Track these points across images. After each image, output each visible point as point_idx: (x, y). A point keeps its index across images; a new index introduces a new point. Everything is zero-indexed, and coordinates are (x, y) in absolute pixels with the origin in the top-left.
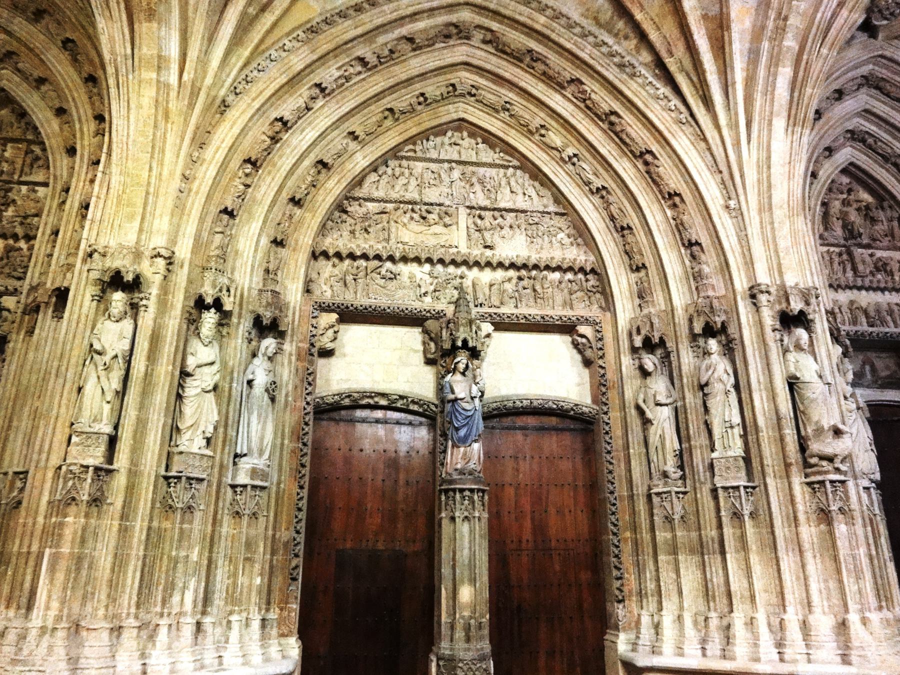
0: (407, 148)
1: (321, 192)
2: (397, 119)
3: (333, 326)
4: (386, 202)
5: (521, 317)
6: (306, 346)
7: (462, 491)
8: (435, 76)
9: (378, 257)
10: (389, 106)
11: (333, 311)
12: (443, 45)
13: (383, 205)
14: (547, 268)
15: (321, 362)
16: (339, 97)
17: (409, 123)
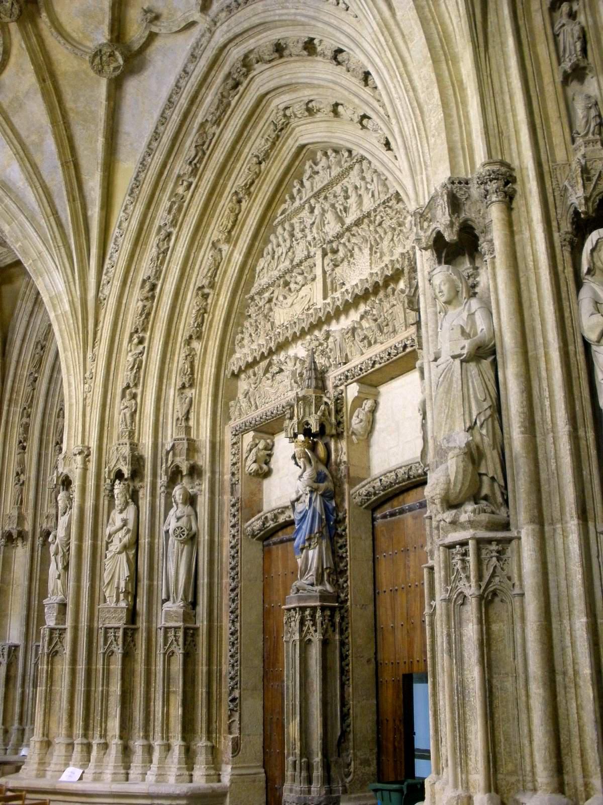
0: (279, 212)
1: (217, 313)
2: (249, 194)
3: (257, 445)
6: (227, 477)
7: (289, 610)
8: (254, 127)
9: (263, 358)
10: (233, 191)
11: (246, 431)
12: (237, 97)
15: (266, 482)
16: (187, 219)
17: (264, 187)
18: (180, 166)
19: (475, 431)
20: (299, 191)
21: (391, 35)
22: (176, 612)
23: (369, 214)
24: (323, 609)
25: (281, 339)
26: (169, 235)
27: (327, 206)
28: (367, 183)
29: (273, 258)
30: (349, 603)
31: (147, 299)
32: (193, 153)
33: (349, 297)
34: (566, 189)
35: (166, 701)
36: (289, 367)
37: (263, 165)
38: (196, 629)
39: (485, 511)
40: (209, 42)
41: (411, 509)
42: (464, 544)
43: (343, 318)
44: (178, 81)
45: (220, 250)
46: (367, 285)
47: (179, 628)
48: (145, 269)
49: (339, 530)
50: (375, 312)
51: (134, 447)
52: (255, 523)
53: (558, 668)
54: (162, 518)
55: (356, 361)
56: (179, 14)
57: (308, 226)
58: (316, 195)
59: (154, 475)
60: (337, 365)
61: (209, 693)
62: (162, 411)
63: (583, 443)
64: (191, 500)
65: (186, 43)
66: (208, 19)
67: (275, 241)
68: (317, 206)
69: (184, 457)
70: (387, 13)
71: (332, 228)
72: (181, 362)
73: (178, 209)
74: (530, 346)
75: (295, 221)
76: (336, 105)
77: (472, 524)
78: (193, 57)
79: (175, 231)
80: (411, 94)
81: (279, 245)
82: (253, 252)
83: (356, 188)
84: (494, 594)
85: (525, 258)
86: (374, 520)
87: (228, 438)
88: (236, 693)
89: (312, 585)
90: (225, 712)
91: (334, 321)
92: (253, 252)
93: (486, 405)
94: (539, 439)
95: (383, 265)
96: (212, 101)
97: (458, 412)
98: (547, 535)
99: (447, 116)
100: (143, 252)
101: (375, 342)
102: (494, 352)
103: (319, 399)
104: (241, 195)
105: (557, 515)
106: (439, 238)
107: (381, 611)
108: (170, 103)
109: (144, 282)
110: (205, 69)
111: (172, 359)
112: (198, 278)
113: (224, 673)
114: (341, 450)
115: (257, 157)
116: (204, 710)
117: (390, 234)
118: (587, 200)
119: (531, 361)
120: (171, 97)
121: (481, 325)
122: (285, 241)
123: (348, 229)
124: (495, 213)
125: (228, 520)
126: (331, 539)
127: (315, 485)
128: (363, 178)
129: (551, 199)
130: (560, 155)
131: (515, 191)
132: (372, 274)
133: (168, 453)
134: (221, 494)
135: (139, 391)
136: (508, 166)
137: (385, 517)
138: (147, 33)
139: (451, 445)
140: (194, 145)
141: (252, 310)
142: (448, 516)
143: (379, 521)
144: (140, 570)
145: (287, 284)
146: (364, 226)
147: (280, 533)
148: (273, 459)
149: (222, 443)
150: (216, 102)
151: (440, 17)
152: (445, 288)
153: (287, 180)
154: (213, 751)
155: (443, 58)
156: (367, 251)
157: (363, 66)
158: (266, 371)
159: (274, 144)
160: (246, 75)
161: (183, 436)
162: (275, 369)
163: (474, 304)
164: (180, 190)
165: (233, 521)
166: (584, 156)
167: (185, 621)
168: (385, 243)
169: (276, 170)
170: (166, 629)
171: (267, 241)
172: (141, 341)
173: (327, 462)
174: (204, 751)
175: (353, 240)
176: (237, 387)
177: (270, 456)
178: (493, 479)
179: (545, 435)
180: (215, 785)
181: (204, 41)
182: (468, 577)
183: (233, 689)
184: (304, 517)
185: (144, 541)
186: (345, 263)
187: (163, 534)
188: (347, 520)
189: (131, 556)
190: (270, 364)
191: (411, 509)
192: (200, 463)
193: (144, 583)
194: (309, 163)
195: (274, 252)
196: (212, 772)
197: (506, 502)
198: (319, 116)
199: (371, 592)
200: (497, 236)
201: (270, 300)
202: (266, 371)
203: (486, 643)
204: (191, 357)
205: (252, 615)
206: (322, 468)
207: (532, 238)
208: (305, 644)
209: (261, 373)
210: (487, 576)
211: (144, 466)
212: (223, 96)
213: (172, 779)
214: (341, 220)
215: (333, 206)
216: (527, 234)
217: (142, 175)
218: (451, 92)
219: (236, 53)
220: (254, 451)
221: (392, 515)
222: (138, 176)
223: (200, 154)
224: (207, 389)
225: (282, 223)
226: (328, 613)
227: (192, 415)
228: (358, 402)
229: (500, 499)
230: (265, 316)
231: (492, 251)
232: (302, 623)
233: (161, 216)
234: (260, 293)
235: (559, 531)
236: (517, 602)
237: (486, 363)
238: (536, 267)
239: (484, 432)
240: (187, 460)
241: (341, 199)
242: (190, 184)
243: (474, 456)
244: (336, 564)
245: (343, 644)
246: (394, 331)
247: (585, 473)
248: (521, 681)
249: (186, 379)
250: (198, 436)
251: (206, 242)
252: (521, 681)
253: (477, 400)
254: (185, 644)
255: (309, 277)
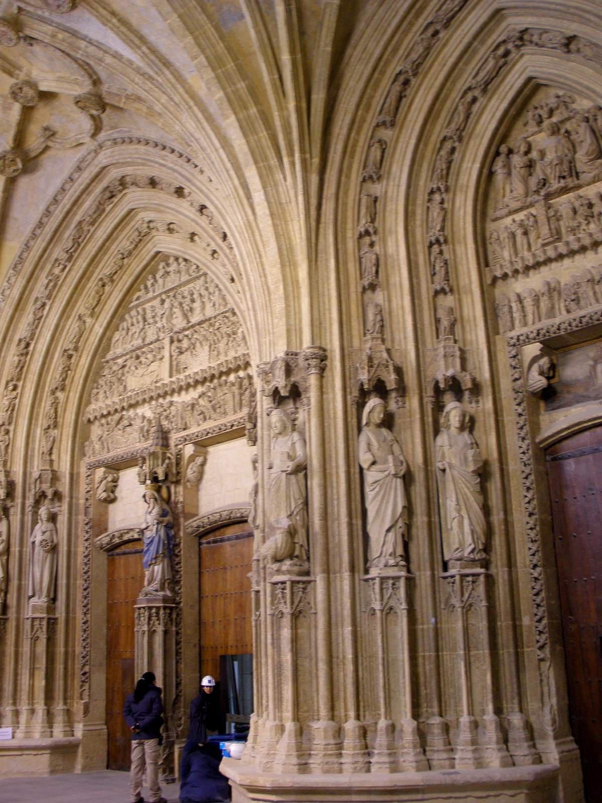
0: (135, 297)
1: (78, 370)
2: (112, 281)
3: (106, 478)
4: (127, 354)
5: (205, 433)
6: (82, 501)
7: (139, 608)
8: (122, 230)
9: (116, 411)
11: (99, 467)
12: (111, 206)
13: (124, 358)
14: (221, 374)
15: (111, 506)
16: (60, 294)
17: (125, 277)
18: (58, 252)
19: (293, 517)
20: (153, 285)
21: (253, 233)
22: (41, 606)
23: (210, 319)
24: (165, 608)
25: (133, 402)
26: (44, 305)
27: (176, 304)
28: (210, 293)
29: (127, 334)
30: (182, 605)
31: (22, 355)
32: (70, 244)
33: (191, 381)
34: (357, 369)
35: (32, 675)
36: (137, 424)
37: (126, 261)
38: (56, 619)
39: (296, 565)
40: (93, 159)
41: (229, 539)
42: (283, 583)
43: (183, 393)
44: (64, 185)
45: (84, 322)
46: (205, 375)
47: (43, 618)
48: (22, 330)
49: (177, 551)
50: (210, 394)
51: (7, 474)
52: (104, 539)
53: (334, 655)
54: (29, 531)
55: (194, 430)
56: (72, 134)
57: (159, 314)
58: (165, 292)
59: (24, 497)
60: (178, 430)
61: (66, 669)
62: (30, 446)
63: (355, 528)
64: (53, 518)
65: (72, 159)
66: (96, 143)
67: (130, 321)
68: (168, 301)
69: (49, 485)
70: (251, 218)
71: (179, 322)
72: (48, 408)
73: (54, 286)
74: (328, 466)
75: (147, 306)
76: (193, 235)
77: (289, 572)
78: (79, 169)
79: (49, 303)
80: (263, 279)
81: (133, 325)
82: (112, 326)
83: (201, 295)
84: (300, 612)
85: (329, 411)
86: (200, 544)
87: (83, 471)
88: (87, 669)
89: (157, 591)
90: (77, 683)
91: (176, 394)
92: (112, 326)
93: (300, 502)
94: (329, 523)
95: (219, 362)
96: (91, 205)
97: (283, 505)
98: (331, 580)
99: (287, 306)
100: (20, 316)
101: (210, 418)
102: (305, 468)
103: (164, 454)
104: (106, 281)
105: (337, 568)
106: (276, 392)
107: (204, 610)
108: (55, 201)
109: (20, 341)
110: (88, 181)
111: (40, 405)
112: (65, 341)
113: (77, 652)
114: (179, 493)
115: (122, 254)
116: (62, 682)
117: (225, 340)
118: (369, 380)
119: (328, 475)
120: (56, 196)
121: (299, 452)
122: (138, 322)
123: (193, 326)
124: (313, 381)
125: (82, 536)
126: (170, 558)
127: (161, 519)
128: (207, 289)
129: (347, 374)
130: (356, 343)
131: (326, 365)
132: (210, 367)
133: (36, 480)
134: (77, 515)
135: (12, 428)
136: (325, 350)
137: (208, 543)
138: (43, 146)
139: (279, 526)
140: (72, 238)
141: (106, 372)
142: (275, 566)
143: (205, 545)
144: (11, 572)
145: (138, 357)
146: (205, 325)
147: (123, 547)
148: (118, 490)
149: (78, 474)
150: (94, 207)
151: (288, 233)
152: (278, 425)
153: (144, 274)
154: (68, 713)
155: (287, 264)
156: (207, 348)
157: (222, 228)
158: (118, 423)
159: (136, 246)
160: (121, 191)
161: (48, 468)
162: (126, 422)
163: (296, 436)
164: (57, 271)
165: (87, 536)
166: (371, 349)
167: (48, 613)
168: (222, 346)
169: (135, 266)
170: (33, 619)
171: (123, 319)
172: (15, 388)
173: (168, 501)
174: (61, 713)
175: (196, 336)
176: (89, 432)
177: (116, 486)
178: (302, 546)
179: (333, 521)
180: (71, 738)
181: (89, 157)
182: (285, 602)
183: (84, 665)
184: (152, 541)
185: (15, 549)
186: (189, 353)
187: (30, 544)
188: (182, 545)
189: (4, 561)
190: (121, 418)
191: (229, 539)
192: (60, 489)
193: (14, 583)
194: (162, 265)
195: (128, 329)
196: (68, 729)
197: (308, 558)
198: (176, 235)
199: (197, 597)
200: (313, 395)
201: (124, 366)
202: (118, 423)
203: (295, 640)
204: (55, 404)
205: (99, 608)
206: (166, 507)
207: (334, 398)
208: (152, 633)
209: (113, 423)
210: (296, 601)
211: (14, 490)
212: (100, 204)
213: (37, 735)
214: (185, 316)
215: (181, 304)
216: (331, 396)
217: (25, 255)
218: (291, 289)
219: (114, 174)
220: (104, 482)
221: (215, 542)
222: (21, 254)
223: (76, 246)
224: (68, 431)
225: (137, 306)
226: (168, 611)
227: (55, 451)
228: (192, 458)
229: (305, 557)
230: (119, 379)
231: (309, 405)
232: (150, 619)
233: (39, 289)
234: (113, 359)
235: (338, 578)
236: (313, 617)
237: (301, 475)
238: (335, 418)
239: (298, 518)
240: (51, 487)
241: (188, 300)
242: (65, 267)
243: (291, 533)
244: (174, 577)
245: (177, 633)
246: (225, 413)
247: (355, 545)
248: (314, 662)
249: (51, 422)
250: (59, 467)
251: (74, 313)
252: (314, 662)
253: (295, 499)
254: (48, 631)
255: (159, 357)
